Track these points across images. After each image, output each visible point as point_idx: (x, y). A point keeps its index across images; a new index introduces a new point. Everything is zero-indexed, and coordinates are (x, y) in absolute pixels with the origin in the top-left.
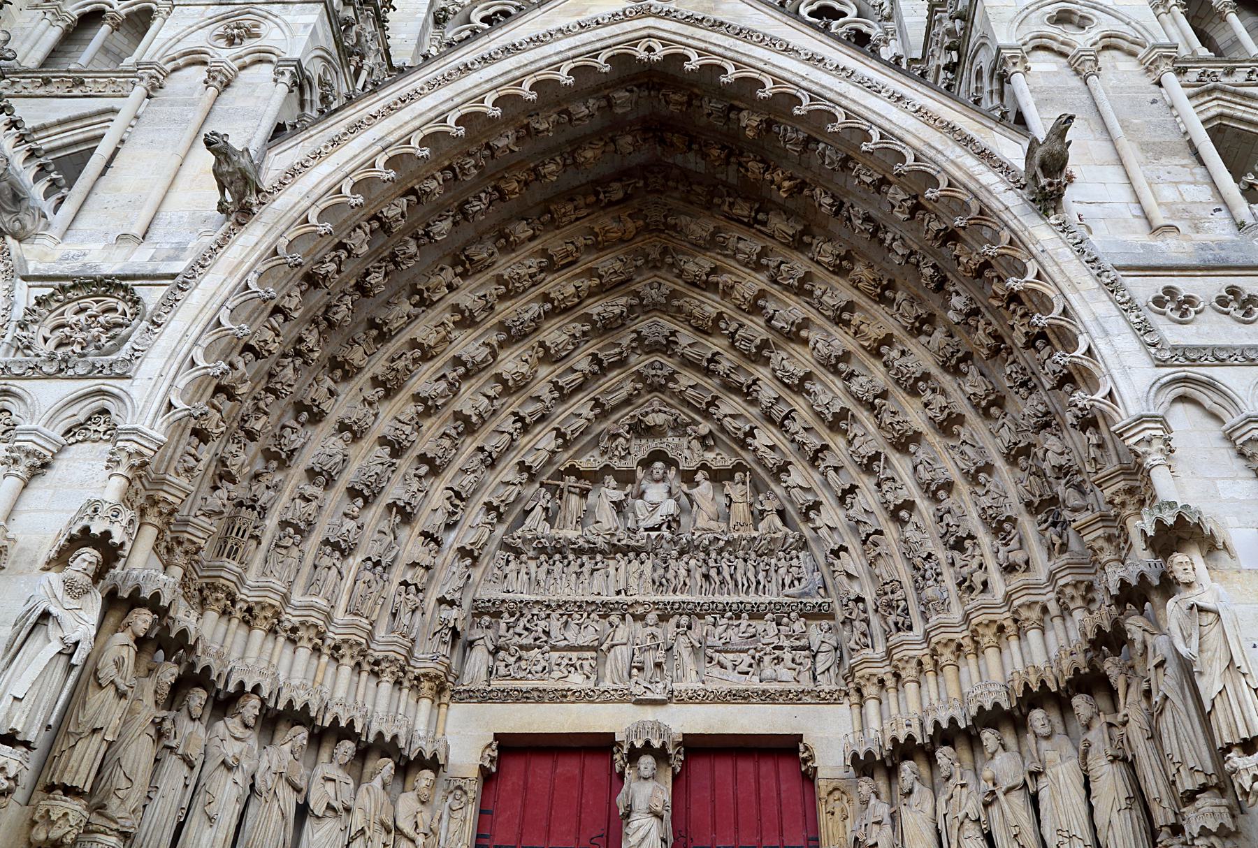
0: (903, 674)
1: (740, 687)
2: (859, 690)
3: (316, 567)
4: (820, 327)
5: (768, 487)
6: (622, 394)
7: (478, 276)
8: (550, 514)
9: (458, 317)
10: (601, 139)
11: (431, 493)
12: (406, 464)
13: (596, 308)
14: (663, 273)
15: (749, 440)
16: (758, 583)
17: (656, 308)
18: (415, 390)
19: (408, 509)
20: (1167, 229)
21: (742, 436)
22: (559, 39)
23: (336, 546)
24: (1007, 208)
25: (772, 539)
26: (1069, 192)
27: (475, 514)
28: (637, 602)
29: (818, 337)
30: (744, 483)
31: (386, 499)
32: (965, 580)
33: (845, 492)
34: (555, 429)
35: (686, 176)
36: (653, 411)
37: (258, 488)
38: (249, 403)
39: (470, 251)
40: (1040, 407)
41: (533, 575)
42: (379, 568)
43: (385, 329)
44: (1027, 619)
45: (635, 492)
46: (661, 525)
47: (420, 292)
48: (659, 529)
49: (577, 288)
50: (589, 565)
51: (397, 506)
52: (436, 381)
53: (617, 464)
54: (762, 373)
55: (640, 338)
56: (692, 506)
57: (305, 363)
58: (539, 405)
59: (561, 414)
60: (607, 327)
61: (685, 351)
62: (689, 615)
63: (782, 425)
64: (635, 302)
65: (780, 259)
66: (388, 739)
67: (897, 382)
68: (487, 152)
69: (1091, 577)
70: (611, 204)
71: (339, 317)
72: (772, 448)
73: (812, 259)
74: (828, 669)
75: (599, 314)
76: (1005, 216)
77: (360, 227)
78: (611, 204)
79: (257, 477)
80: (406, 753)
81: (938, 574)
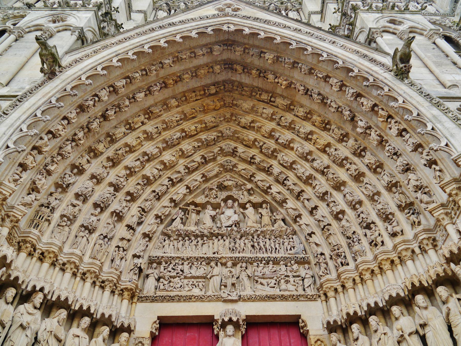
0: (347, 285)
1: (271, 293)
2: (325, 294)
3: (76, 236)
4: (299, 142)
5: (277, 209)
6: (214, 173)
7: (155, 120)
9: (145, 136)
10: (207, 66)
11: (131, 209)
12: (121, 195)
13: (203, 136)
14: (231, 124)
15: (269, 190)
16: (276, 249)
17: (229, 138)
18: (126, 164)
19: (121, 214)
20: (454, 86)
21: (266, 189)
22: (191, 22)
23: (86, 228)
24: (386, 78)
26: (412, 70)
27: (150, 219)
28: (222, 257)
29: (298, 146)
30: (267, 208)
31: (111, 209)
32: (373, 241)
34: (186, 185)
35: (241, 85)
36: (227, 180)
37: (51, 199)
38: (49, 159)
39: (152, 109)
40: (405, 162)
41: (176, 247)
42: (106, 239)
43: (114, 137)
44: (406, 256)
45: (220, 212)
46: (232, 225)
47: (130, 124)
48: (231, 226)
49: (196, 127)
50: (201, 242)
51: (116, 213)
52: (136, 161)
53: (212, 201)
54: (274, 163)
55: (221, 149)
56: (245, 217)
57: (77, 145)
58: (179, 175)
59: (188, 180)
60: (207, 144)
61: (241, 155)
62: (246, 263)
63: (283, 183)
64: (220, 135)
65: (281, 115)
66: (107, 316)
67: (334, 162)
68: (161, 65)
69: (435, 235)
70: (211, 95)
71: (93, 127)
72: (279, 193)
73: (295, 115)
74: (310, 286)
75: (205, 139)
76: (385, 81)
77: (105, 89)
78: (211, 95)
79: (51, 194)
80: (115, 324)
81: (359, 240)
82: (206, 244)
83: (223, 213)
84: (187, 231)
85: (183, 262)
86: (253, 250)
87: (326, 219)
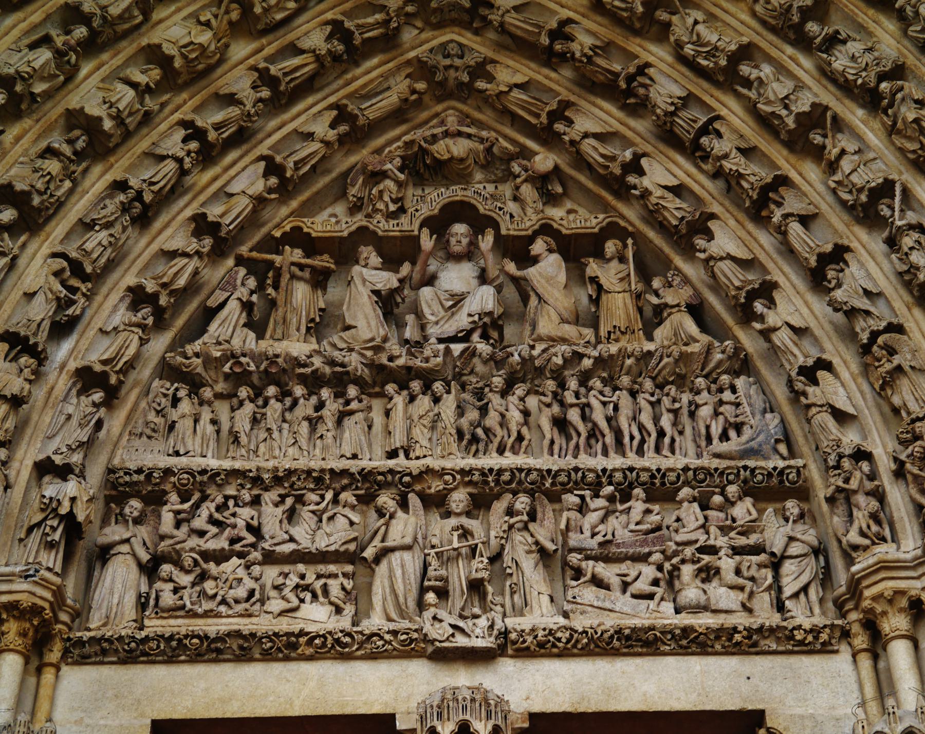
1: (637, 622)
5: (668, 264)
6: (390, 100)
8: (257, 315)
11: (22, 262)
15: (632, 179)
16: (661, 434)
21: (618, 171)
25: (682, 354)
28: (429, 471)
30: (622, 259)
33: (825, 260)
36: (446, 134)
41: (225, 426)
45: (416, 276)
46: (470, 333)
50: (332, 407)
52: (33, 46)
53: (382, 226)
56: (525, 299)
58: (233, 112)
61: (507, 19)
62: (531, 493)
72: (678, 190)
74: (805, 589)
82: (359, 416)
83: (430, 280)
84: (273, 360)
85: (255, 492)
86: (560, 441)
87: (881, 303)
